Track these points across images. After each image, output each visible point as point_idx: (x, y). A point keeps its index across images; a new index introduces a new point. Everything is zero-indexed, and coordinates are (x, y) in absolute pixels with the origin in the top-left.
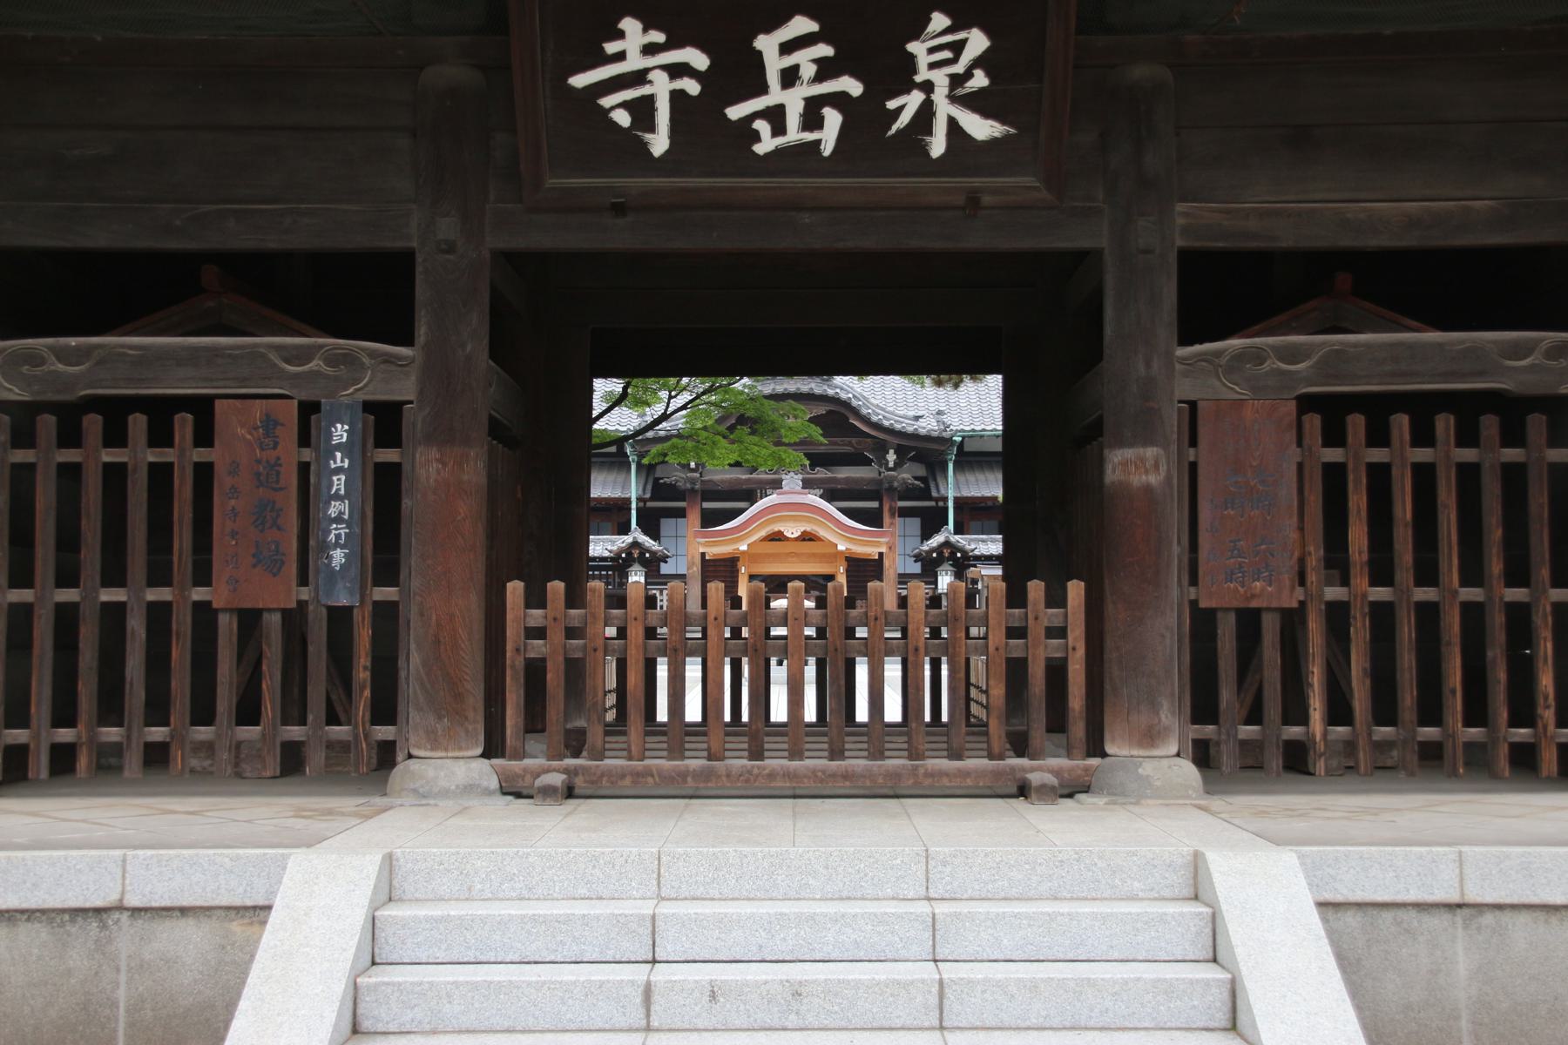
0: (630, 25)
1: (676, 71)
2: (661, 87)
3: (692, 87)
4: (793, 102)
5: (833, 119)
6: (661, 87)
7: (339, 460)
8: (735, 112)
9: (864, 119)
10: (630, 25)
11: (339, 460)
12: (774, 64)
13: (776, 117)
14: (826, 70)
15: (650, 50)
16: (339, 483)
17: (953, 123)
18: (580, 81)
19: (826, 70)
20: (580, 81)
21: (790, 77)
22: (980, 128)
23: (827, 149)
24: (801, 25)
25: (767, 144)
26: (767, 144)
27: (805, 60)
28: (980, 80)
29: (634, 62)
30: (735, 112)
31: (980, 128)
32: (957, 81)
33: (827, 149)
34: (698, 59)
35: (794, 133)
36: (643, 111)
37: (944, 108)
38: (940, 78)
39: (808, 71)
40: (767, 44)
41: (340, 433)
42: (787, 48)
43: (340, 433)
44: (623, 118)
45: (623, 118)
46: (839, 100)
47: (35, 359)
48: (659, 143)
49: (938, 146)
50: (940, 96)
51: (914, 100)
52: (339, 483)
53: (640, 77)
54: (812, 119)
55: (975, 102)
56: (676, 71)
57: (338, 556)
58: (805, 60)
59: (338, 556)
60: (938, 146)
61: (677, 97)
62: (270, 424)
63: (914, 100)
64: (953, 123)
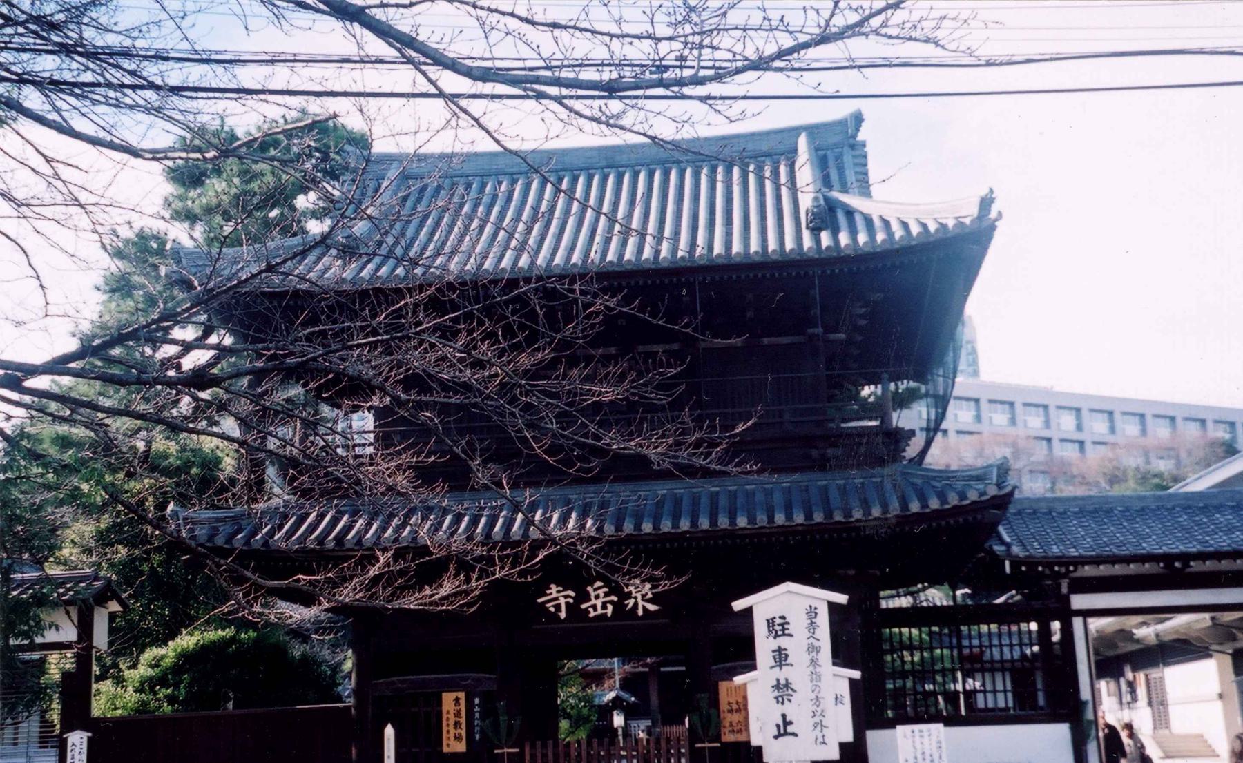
0: (553, 586)
1: (566, 597)
2: (562, 601)
3: (571, 601)
4: (599, 603)
5: (610, 607)
6: (562, 601)
7: (477, 709)
8: (583, 606)
9: (619, 607)
10: (553, 586)
11: (477, 709)
12: (593, 594)
13: (594, 607)
14: (606, 594)
15: (558, 592)
16: (477, 715)
17: (644, 607)
18: (540, 600)
19: (606, 594)
20: (540, 600)
21: (597, 597)
22: (652, 607)
23: (609, 614)
24: (599, 584)
25: (592, 614)
26: (592, 614)
27: (601, 592)
28: (650, 595)
29: (555, 595)
30: (583, 606)
31: (652, 607)
32: (643, 596)
33: (609, 614)
34: (572, 594)
35: (600, 611)
36: (558, 607)
37: (641, 603)
38: (639, 595)
39: (602, 595)
40: (589, 589)
41: (477, 701)
42: (595, 590)
43: (477, 701)
44: (552, 609)
45: (552, 609)
46: (611, 602)
47: (393, 683)
48: (563, 615)
49: (640, 612)
50: (639, 600)
51: (632, 602)
52: (477, 715)
53: (557, 599)
54: (604, 606)
55: (649, 601)
56: (566, 597)
57: (477, 737)
58: (601, 592)
59: (477, 737)
60: (640, 612)
61: (567, 603)
62: (457, 700)
63: (632, 602)
64: (644, 607)
